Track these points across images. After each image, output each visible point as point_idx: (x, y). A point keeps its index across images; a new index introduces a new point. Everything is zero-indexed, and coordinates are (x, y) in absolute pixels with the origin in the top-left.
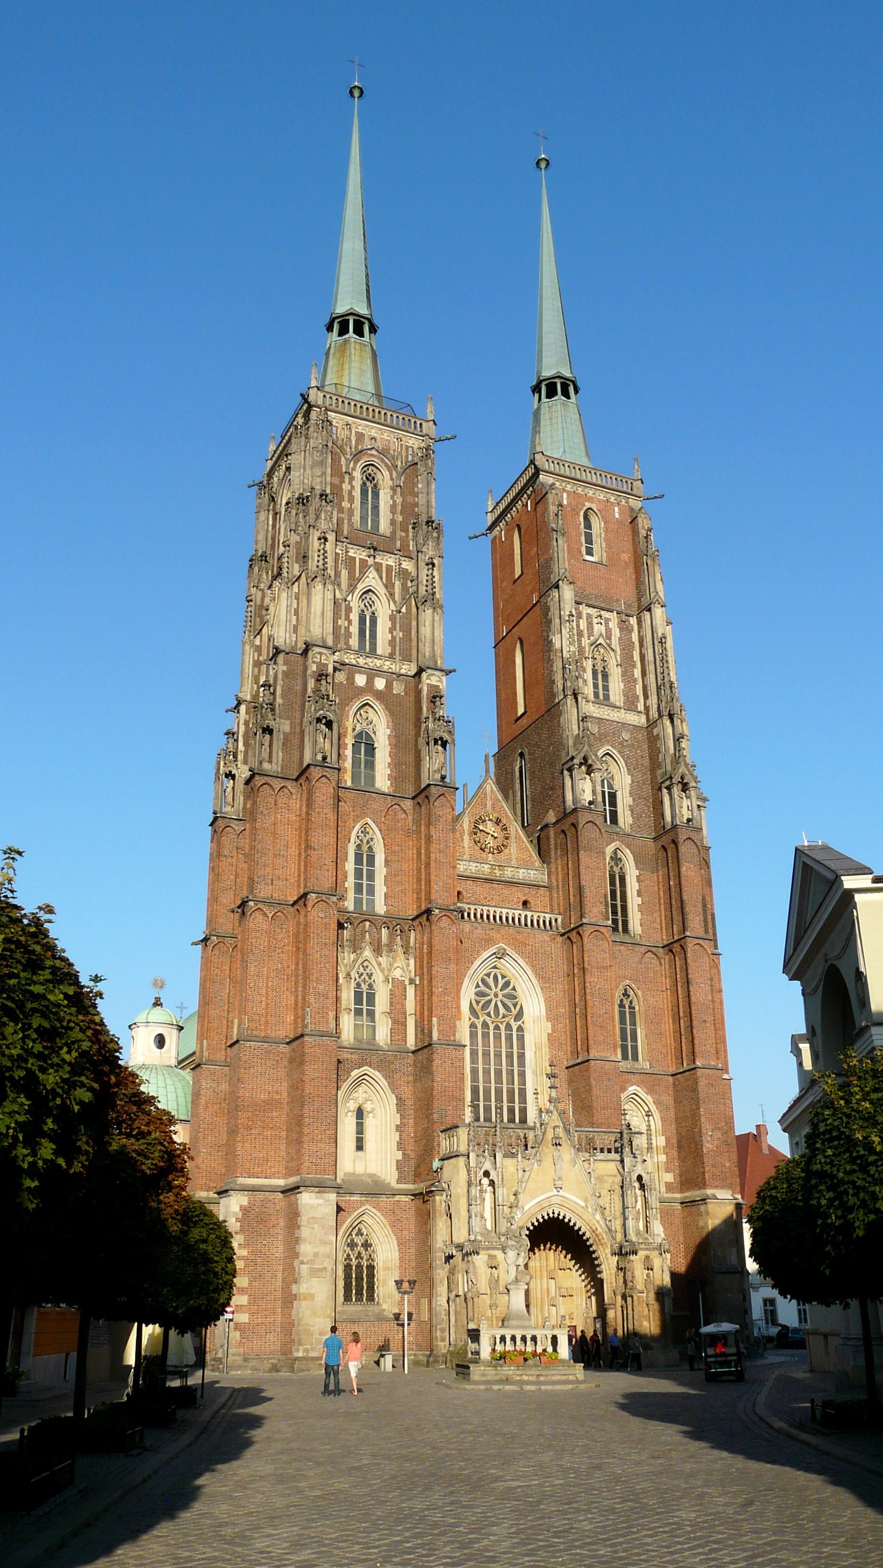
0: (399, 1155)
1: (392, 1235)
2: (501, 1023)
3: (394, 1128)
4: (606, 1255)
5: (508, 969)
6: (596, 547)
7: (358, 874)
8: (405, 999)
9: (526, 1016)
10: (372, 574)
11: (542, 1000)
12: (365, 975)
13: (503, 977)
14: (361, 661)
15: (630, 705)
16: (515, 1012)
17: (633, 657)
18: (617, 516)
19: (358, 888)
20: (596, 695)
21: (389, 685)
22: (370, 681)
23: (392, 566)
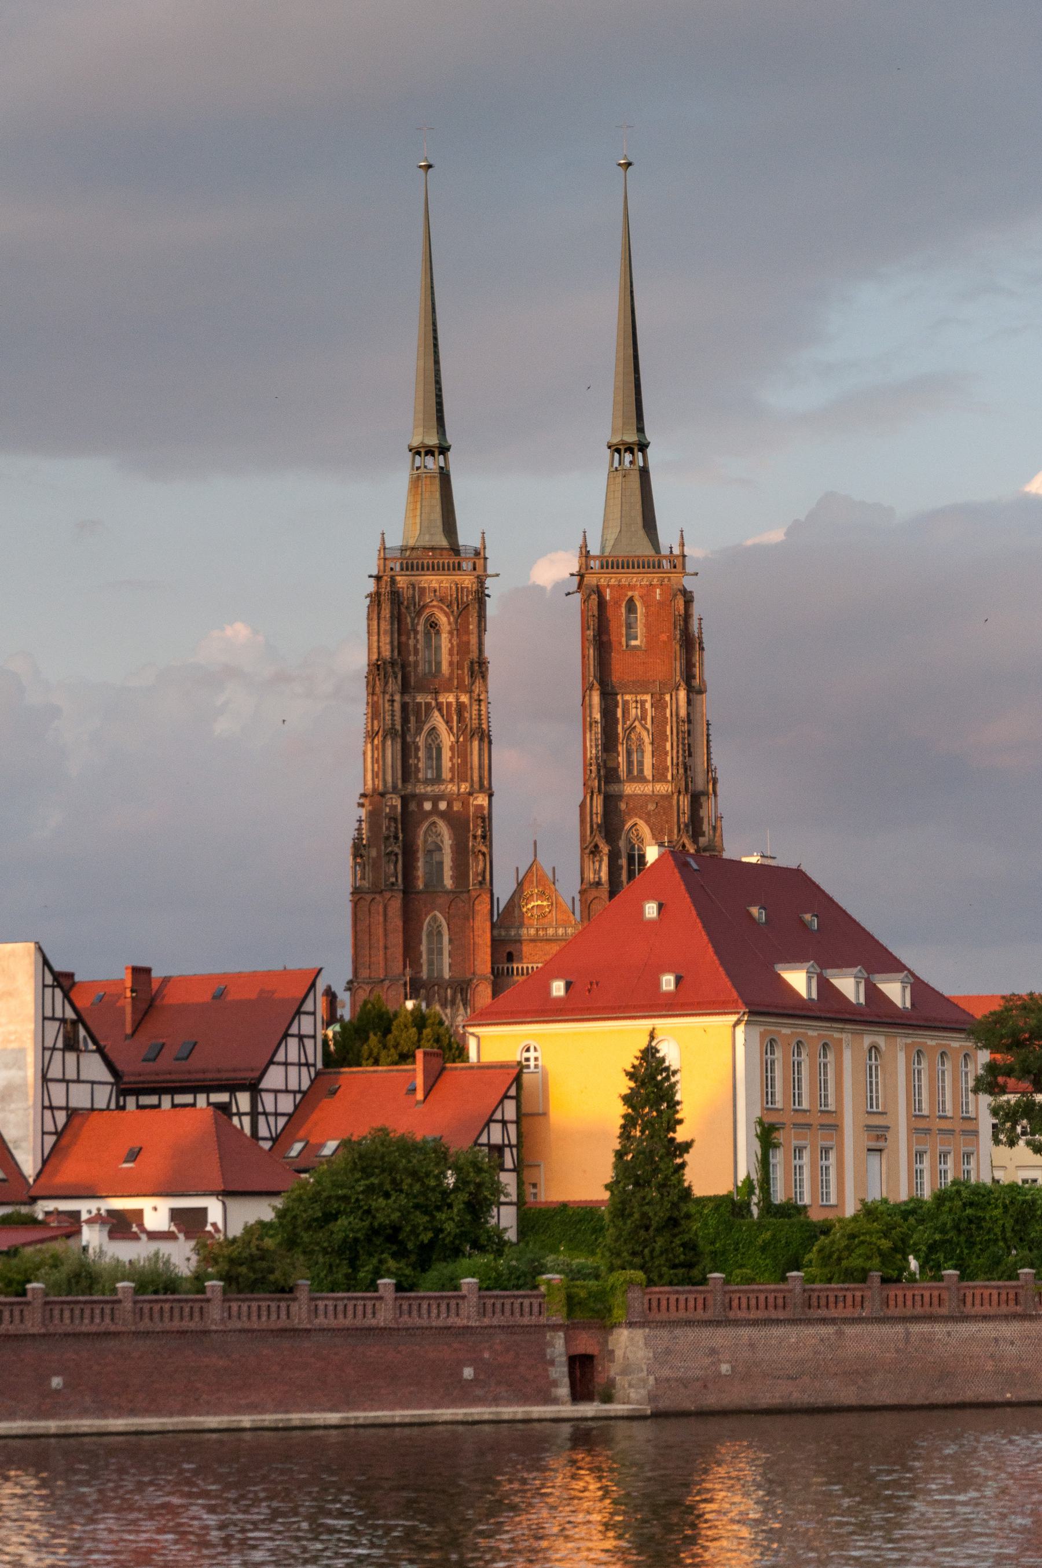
6: (640, 629)
7: (430, 951)
10: (436, 713)
14: (429, 789)
15: (659, 775)
18: (658, 597)
19: (431, 963)
20: (630, 771)
21: (450, 805)
22: (435, 805)
23: (451, 703)
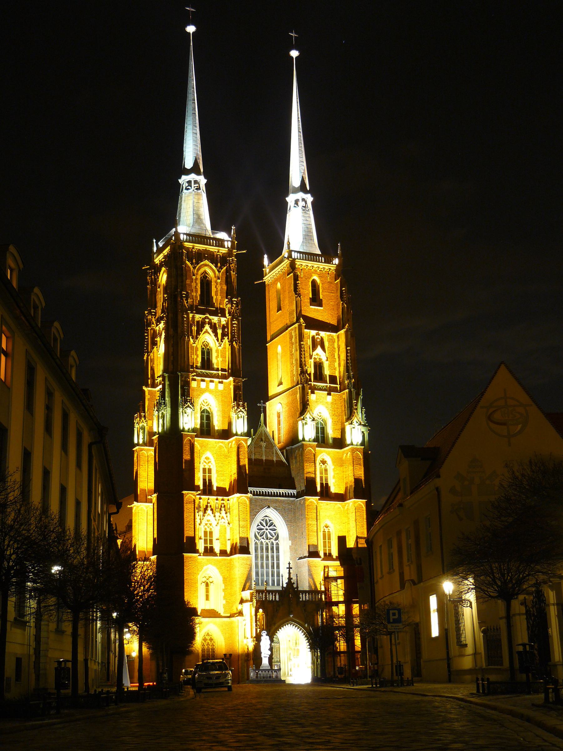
0: (224, 602)
3: (222, 590)
12: (208, 525)
17: (334, 356)
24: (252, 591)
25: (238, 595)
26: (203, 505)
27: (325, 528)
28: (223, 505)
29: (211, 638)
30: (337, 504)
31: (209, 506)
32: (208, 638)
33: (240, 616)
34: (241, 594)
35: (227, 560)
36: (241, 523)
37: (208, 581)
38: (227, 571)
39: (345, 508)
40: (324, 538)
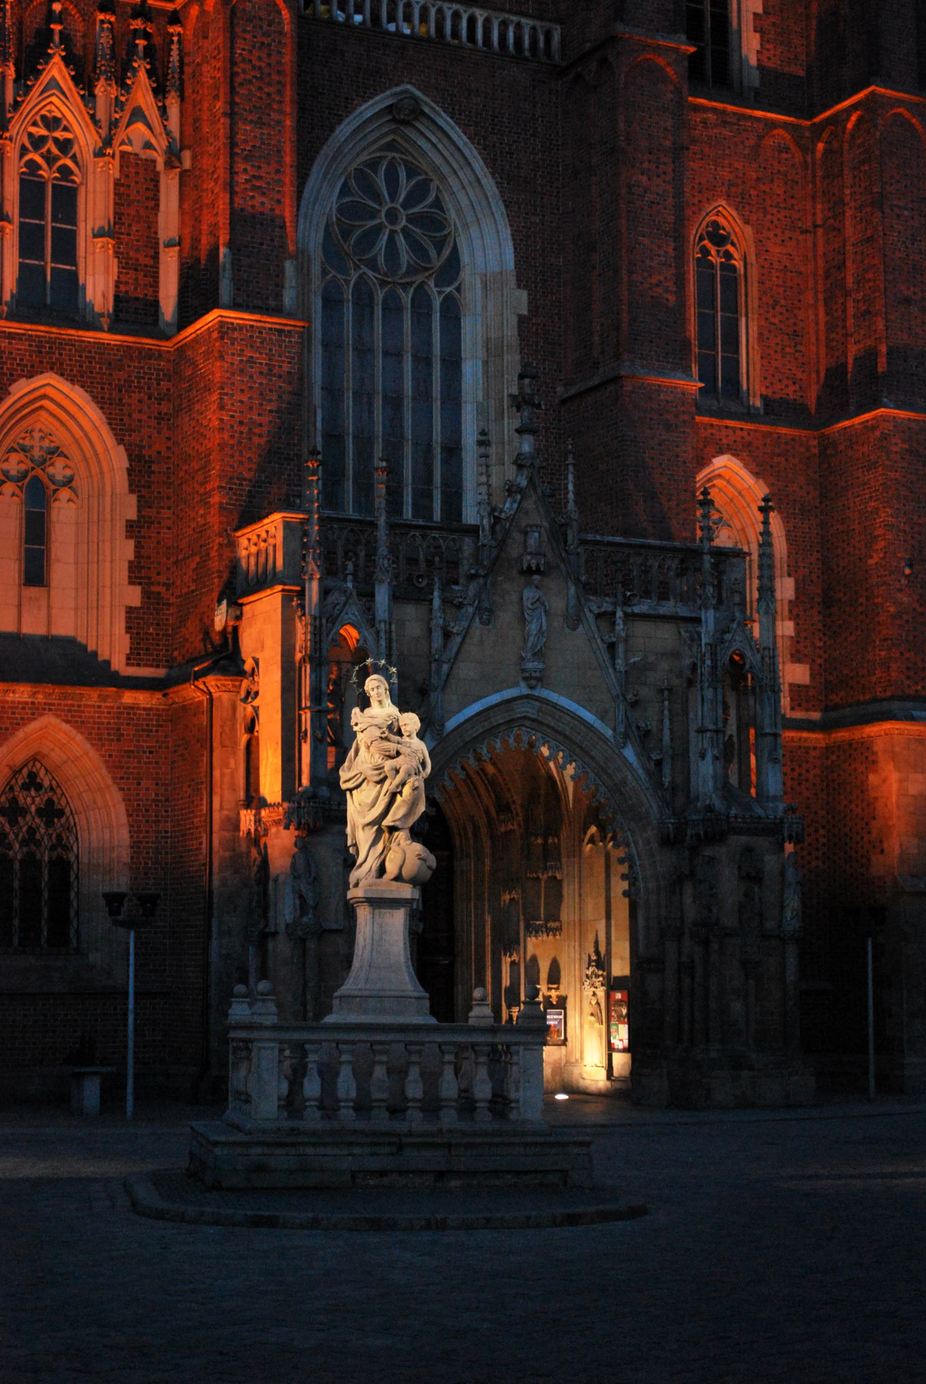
0: (134, 596)
1: (114, 789)
2: (405, 286)
3: (120, 528)
4: (648, 842)
5: (424, 154)
8: (157, 207)
9: (466, 275)
11: (506, 233)
12: (50, 145)
13: (412, 172)
16: (438, 261)
24: (295, 517)
25: (213, 554)
26: (20, 24)
27: (706, 242)
28: (141, 43)
29: (50, 802)
30: (773, 124)
31: (57, 38)
32: (32, 801)
33: (224, 671)
34: (232, 545)
35: (160, 355)
36: (245, 130)
37: (38, 472)
38: (154, 423)
39: (814, 153)
40: (706, 299)
